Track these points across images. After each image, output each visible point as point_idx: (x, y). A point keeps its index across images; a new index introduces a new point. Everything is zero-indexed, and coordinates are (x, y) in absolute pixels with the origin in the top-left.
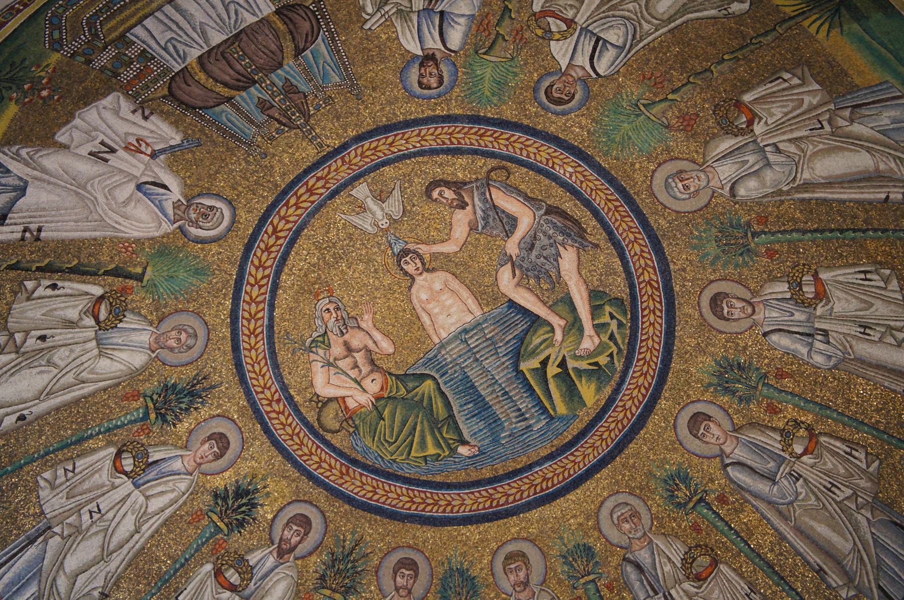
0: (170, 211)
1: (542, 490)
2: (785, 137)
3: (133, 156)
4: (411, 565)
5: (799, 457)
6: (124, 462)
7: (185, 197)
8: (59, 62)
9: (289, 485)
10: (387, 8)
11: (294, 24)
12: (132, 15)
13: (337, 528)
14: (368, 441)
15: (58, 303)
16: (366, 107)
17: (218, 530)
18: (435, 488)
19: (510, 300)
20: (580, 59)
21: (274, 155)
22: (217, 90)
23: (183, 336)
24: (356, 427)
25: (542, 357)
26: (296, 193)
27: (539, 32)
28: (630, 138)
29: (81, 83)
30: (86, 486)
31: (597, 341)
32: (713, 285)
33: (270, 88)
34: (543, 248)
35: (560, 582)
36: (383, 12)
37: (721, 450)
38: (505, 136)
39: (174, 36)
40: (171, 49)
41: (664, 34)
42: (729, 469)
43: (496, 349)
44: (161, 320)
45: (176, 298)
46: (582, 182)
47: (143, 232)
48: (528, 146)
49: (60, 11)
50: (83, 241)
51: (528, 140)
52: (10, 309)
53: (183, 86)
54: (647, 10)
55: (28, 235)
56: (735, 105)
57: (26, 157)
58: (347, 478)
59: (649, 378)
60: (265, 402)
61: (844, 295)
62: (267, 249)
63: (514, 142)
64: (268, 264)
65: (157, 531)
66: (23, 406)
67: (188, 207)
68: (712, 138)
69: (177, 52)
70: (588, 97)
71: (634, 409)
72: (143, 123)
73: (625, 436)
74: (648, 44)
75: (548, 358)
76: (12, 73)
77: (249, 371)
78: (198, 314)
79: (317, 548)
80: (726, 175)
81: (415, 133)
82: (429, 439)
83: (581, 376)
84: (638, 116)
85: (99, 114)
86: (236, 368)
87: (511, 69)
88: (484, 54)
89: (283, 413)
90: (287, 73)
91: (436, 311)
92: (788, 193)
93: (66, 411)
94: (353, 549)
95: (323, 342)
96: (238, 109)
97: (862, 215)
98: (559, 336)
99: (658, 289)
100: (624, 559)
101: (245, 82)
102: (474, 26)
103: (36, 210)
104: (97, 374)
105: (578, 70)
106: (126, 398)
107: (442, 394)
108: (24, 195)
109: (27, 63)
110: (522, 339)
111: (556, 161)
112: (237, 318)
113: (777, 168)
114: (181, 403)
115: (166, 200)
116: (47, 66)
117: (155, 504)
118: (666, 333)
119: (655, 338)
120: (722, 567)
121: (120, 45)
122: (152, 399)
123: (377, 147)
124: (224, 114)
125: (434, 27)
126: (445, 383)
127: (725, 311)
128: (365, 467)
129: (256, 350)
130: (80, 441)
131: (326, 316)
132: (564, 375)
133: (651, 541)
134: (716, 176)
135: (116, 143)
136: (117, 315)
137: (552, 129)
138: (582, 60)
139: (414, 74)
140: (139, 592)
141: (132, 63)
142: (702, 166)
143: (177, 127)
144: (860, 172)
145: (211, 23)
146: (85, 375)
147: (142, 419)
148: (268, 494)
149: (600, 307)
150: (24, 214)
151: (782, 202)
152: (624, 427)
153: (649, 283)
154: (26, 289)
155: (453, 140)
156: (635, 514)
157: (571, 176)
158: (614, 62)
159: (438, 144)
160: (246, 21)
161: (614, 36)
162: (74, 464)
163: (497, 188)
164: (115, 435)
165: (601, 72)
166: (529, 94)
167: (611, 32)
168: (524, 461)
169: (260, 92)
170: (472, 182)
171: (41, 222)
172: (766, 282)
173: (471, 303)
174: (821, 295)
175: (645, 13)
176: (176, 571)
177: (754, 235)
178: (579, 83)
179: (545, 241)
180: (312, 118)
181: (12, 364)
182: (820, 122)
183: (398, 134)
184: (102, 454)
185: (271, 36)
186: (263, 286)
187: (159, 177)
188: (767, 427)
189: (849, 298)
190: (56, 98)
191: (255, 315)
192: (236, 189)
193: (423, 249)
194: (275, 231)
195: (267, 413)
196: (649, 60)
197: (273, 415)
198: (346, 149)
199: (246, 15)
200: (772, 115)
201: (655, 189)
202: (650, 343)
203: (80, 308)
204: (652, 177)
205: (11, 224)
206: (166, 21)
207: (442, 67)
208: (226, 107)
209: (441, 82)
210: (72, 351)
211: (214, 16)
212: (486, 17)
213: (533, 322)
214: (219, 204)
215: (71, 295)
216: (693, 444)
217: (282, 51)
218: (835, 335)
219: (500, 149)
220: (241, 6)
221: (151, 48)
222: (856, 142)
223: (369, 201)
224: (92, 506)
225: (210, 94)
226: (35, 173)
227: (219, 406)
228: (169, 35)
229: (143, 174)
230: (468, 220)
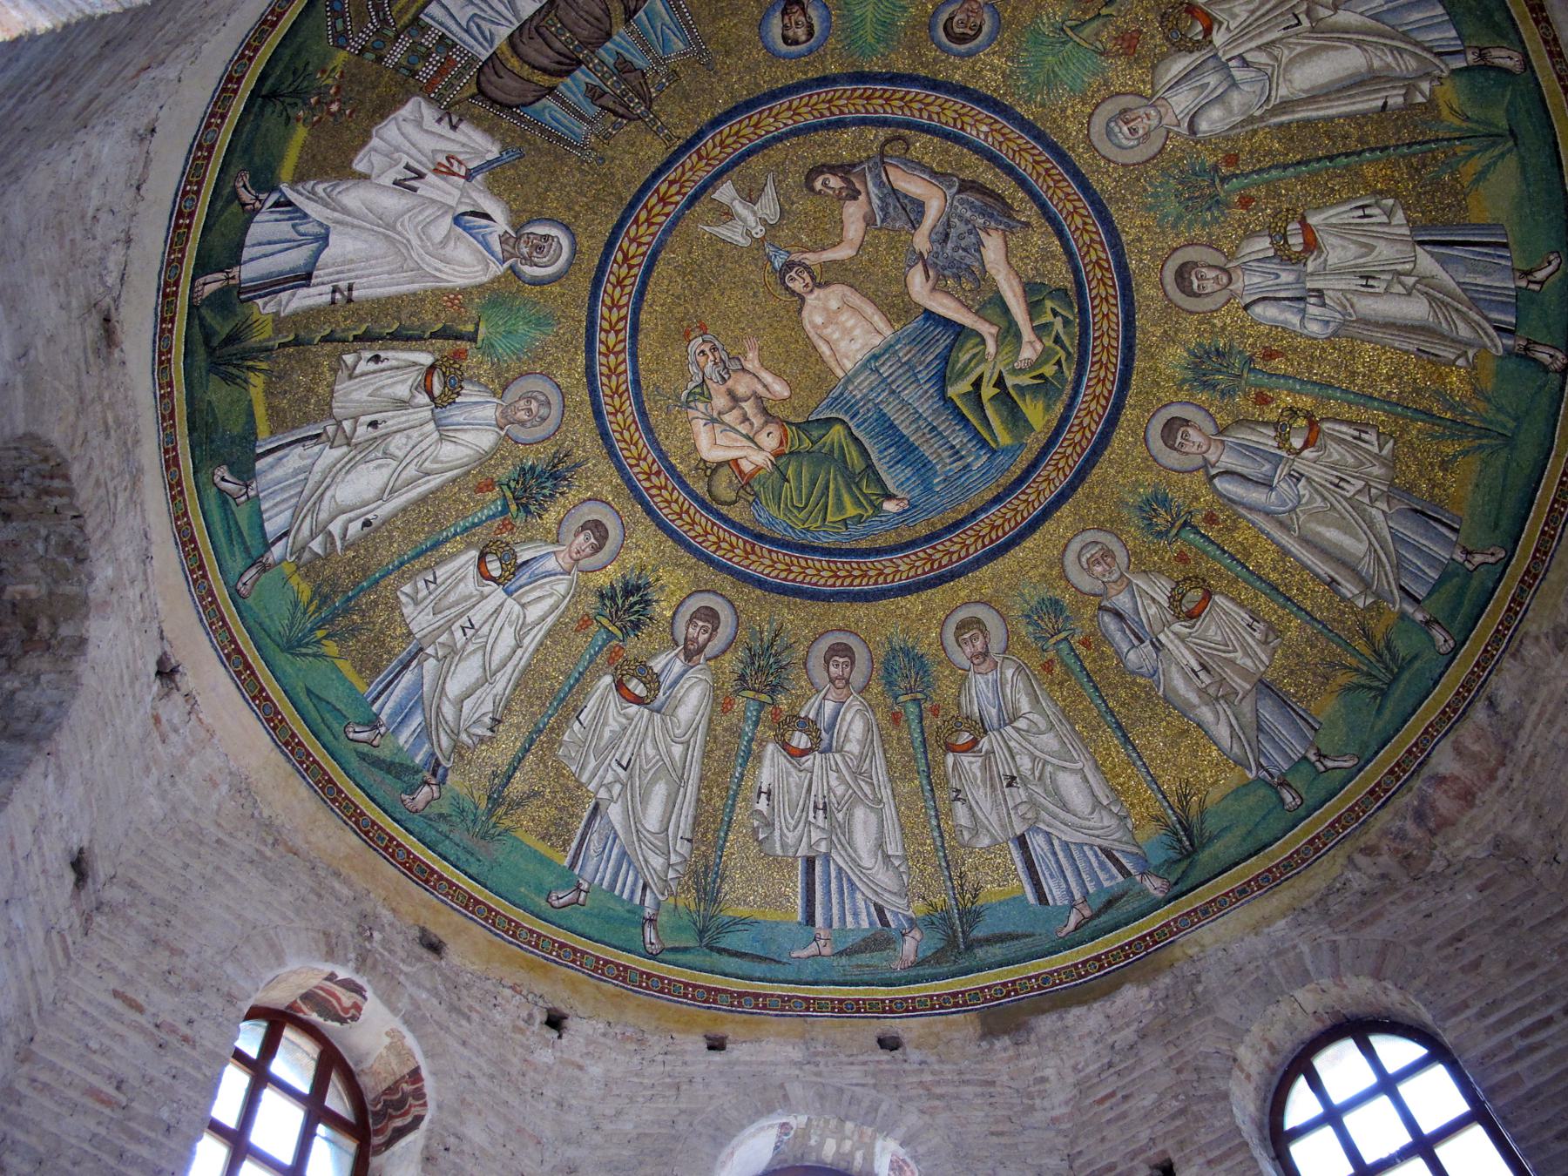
0: (497, 248)
1: (992, 541)
2: (1253, 44)
4: (846, 651)
5: (1298, 453)
6: (490, 567)
7: (513, 226)
8: (346, 63)
9: (686, 574)
13: (751, 619)
14: (773, 510)
15: (385, 379)
16: (721, 80)
17: (612, 636)
18: (861, 556)
19: (926, 310)
21: (613, 159)
22: (535, 79)
24: (756, 494)
25: (973, 377)
26: (645, 206)
28: (1056, 75)
29: (374, 88)
30: (452, 598)
31: (1039, 347)
32: (1178, 253)
34: (960, 237)
35: (1026, 646)
37: (1205, 459)
38: (898, 95)
39: (477, 11)
42: (1216, 481)
43: (915, 375)
44: (505, 388)
45: (519, 359)
46: (1001, 143)
50: (400, 297)
52: (332, 391)
53: (494, 78)
55: (338, 296)
56: (1187, 11)
58: (753, 557)
59: (1108, 385)
60: (642, 477)
61: (1340, 242)
62: (620, 283)
64: (624, 300)
65: (541, 644)
67: (518, 239)
69: (482, 33)
70: (998, 27)
71: (1093, 427)
72: (451, 134)
73: (1087, 460)
75: (981, 377)
78: (548, 376)
79: (730, 645)
82: (847, 499)
83: (1023, 396)
84: (1064, 43)
89: (666, 488)
90: (618, 45)
91: (836, 336)
92: (1262, 118)
94: (774, 640)
95: (702, 394)
96: (563, 103)
97: (1355, 134)
98: (991, 347)
99: (1108, 270)
100: (1100, 608)
103: (343, 263)
106: (479, 489)
107: (856, 439)
109: (310, 68)
110: (945, 359)
111: (966, 119)
112: (595, 376)
113: (1246, 88)
116: (333, 70)
117: (534, 613)
118: (1124, 324)
119: (1113, 334)
120: (1216, 598)
121: (414, 32)
126: (858, 426)
127: (1195, 286)
128: (773, 541)
130: (436, 545)
131: (701, 359)
132: (1004, 396)
133: (1130, 582)
136: (453, 389)
139: (776, 26)
140: (534, 714)
141: (430, 55)
142: (1151, 100)
143: (493, 136)
144: (1351, 76)
148: (662, 588)
149: (1039, 303)
151: (1255, 132)
152: (1083, 450)
153: (1097, 262)
155: (836, 111)
156: (1108, 553)
166: (923, 34)
168: (966, 508)
172: (1242, 239)
173: (879, 321)
174: (1311, 245)
176: (571, 687)
177: (1224, 180)
179: (962, 228)
182: (1296, 16)
184: (463, 559)
188: (1257, 422)
189: (1346, 243)
193: (811, 258)
194: (626, 258)
195: (647, 489)
197: (654, 491)
200: (1234, 16)
201: (1094, 138)
202: (1106, 340)
207: (810, 11)
208: (548, 102)
209: (810, 34)
210: (408, 437)
213: (958, 334)
214: (554, 232)
216: (1171, 458)
217: (609, 16)
218: (1330, 293)
222: (1342, 36)
223: (736, 203)
224: (465, 618)
225: (527, 85)
226: (336, 215)
227: (588, 488)
228: (471, 10)
229: (459, 202)
230: (860, 215)
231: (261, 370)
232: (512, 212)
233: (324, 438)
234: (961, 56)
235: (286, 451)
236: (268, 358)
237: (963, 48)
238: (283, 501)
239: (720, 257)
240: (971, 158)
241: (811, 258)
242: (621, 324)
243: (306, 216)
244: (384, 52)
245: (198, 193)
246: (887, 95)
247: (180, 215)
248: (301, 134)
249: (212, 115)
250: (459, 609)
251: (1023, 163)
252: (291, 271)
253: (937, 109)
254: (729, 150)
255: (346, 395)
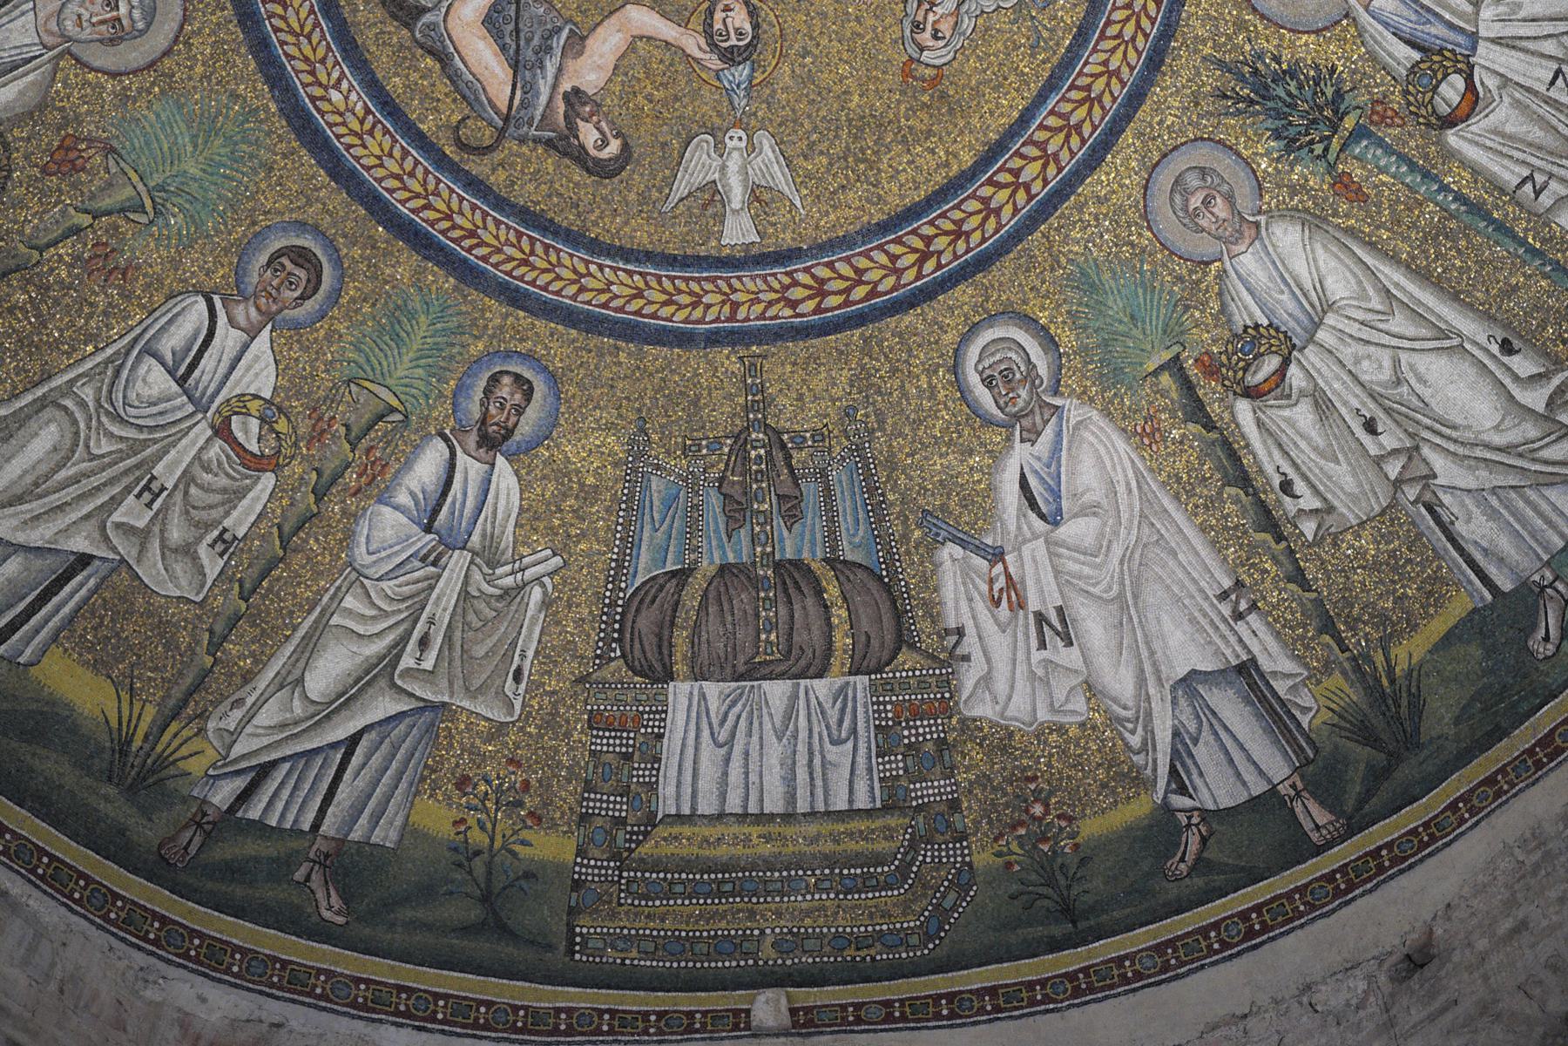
0: (1048, 433)
3: (1023, 582)
6: (1456, 99)
7: (1009, 439)
10: (509, 581)
11: (660, 637)
12: (851, 835)
15: (1305, 454)
20: (230, 343)
23: (1196, 201)
26: (847, 303)
27: (282, 425)
28: (194, 137)
30: (1537, 134)
33: (762, 537)
36: (519, 576)
38: (431, 215)
39: (828, 745)
40: (846, 724)
41: (61, 371)
46: (323, 61)
47: (1108, 437)
48: (397, 177)
49: (914, 940)
51: (391, 191)
52: (1362, 524)
53: (875, 643)
54: (77, 433)
57: (1140, 730)
62: (958, 234)
63: (418, 196)
64: (974, 205)
66: (1487, 361)
67: (1017, 417)
68: (31, 114)
70: (244, 251)
72: (970, 630)
74: (97, 349)
76: (1041, 890)
77: (1146, 36)
80: (19, 22)
81: (586, 296)
85: (1010, 698)
86: (1162, 62)
87: (362, 360)
88: (393, 410)
90: (721, 547)
93: (1449, 280)
101: (792, 575)
102: (388, 476)
104: (1360, 283)
105: (241, 320)
108: (1194, 672)
109: (1015, 887)
111: (356, 126)
112: (1093, 149)
114: (1289, 94)
115: (1039, 459)
116: (999, 854)
121: (901, 792)
122: (1326, 149)
123: (665, 304)
124: (857, 540)
125: (454, 503)
129: (1105, 63)
130: (1476, 209)
131: (946, 28)
134: (41, 21)
135: (1027, 626)
136: (1256, 339)
137: (337, 199)
138: (228, 338)
141: (910, 746)
142: (66, 53)
145: (768, 726)
146: (1376, 303)
147: (1369, 135)
150: (1219, 641)
154: (1319, 527)
157: (339, 81)
158: (170, 322)
159: (558, 251)
160: (721, 693)
161: (155, 380)
162: (1519, 186)
163: (493, 106)
164: (1426, 157)
165: (202, 305)
167: (155, 392)
169: (782, 540)
170: (536, 141)
171: (1212, 605)
175: (82, 425)
178: (250, 289)
180: (736, 430)
181: (1438, 440)
183: (616, 310)
184: (1472, 153)
185: (704, 638)
186: (1010, 171)
187: (1019, 509)
190: (1033, 786)
191: (1060, 129)
192: (929, 383)
193: (693, 43)
194: (924, 257)
196: (105, 313)
198: (717, 332)
199: (713, 704)
203: (1286, 413)
204: (176, 41)
205: (1245, 647)
206: (819, 783)
207: (477, 416)
209: (495, 379)
211: (755, 738)
212: (358, 491)
214: (974, 379)
215: (1280, 446)
219: (452, 191)
220: (711, 728)
221: (869, 748)
223: (736, 205)
226: (1152, 691)
227: (1240, 25)
228: (832, 752)
229: (1036, 537)
231: (1387, 660)
232: (997, 457)
233: (1428, 496)
234: (316, 230)
235: (1471, 549)
236: (1369, 659)
237: (306, 241)
238: (1541, 514)
239: (811, 145)
240: (382, 63)
241: (693, 43)
242: (1005, 178)
243: (1176, 734)
244: (943, 808)
245: (1216, 926)
246: (445, 225)
247: (1250, 934)
248: (1091, 827)
249: (1125, 980)
250: (1545, 110)
251: (303, 14)
252: (1248, 702)
253: (387, 162)
254: (695, 287)
255: (1355, 499)
